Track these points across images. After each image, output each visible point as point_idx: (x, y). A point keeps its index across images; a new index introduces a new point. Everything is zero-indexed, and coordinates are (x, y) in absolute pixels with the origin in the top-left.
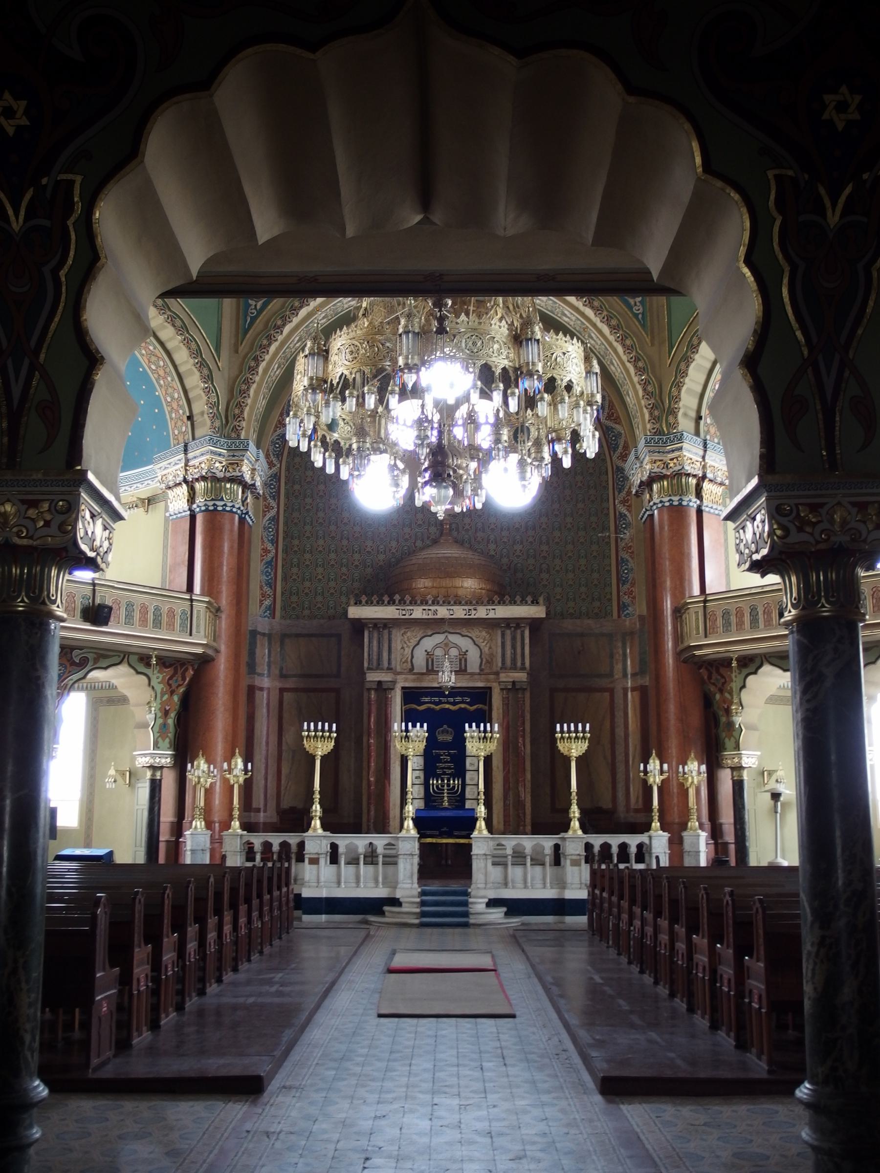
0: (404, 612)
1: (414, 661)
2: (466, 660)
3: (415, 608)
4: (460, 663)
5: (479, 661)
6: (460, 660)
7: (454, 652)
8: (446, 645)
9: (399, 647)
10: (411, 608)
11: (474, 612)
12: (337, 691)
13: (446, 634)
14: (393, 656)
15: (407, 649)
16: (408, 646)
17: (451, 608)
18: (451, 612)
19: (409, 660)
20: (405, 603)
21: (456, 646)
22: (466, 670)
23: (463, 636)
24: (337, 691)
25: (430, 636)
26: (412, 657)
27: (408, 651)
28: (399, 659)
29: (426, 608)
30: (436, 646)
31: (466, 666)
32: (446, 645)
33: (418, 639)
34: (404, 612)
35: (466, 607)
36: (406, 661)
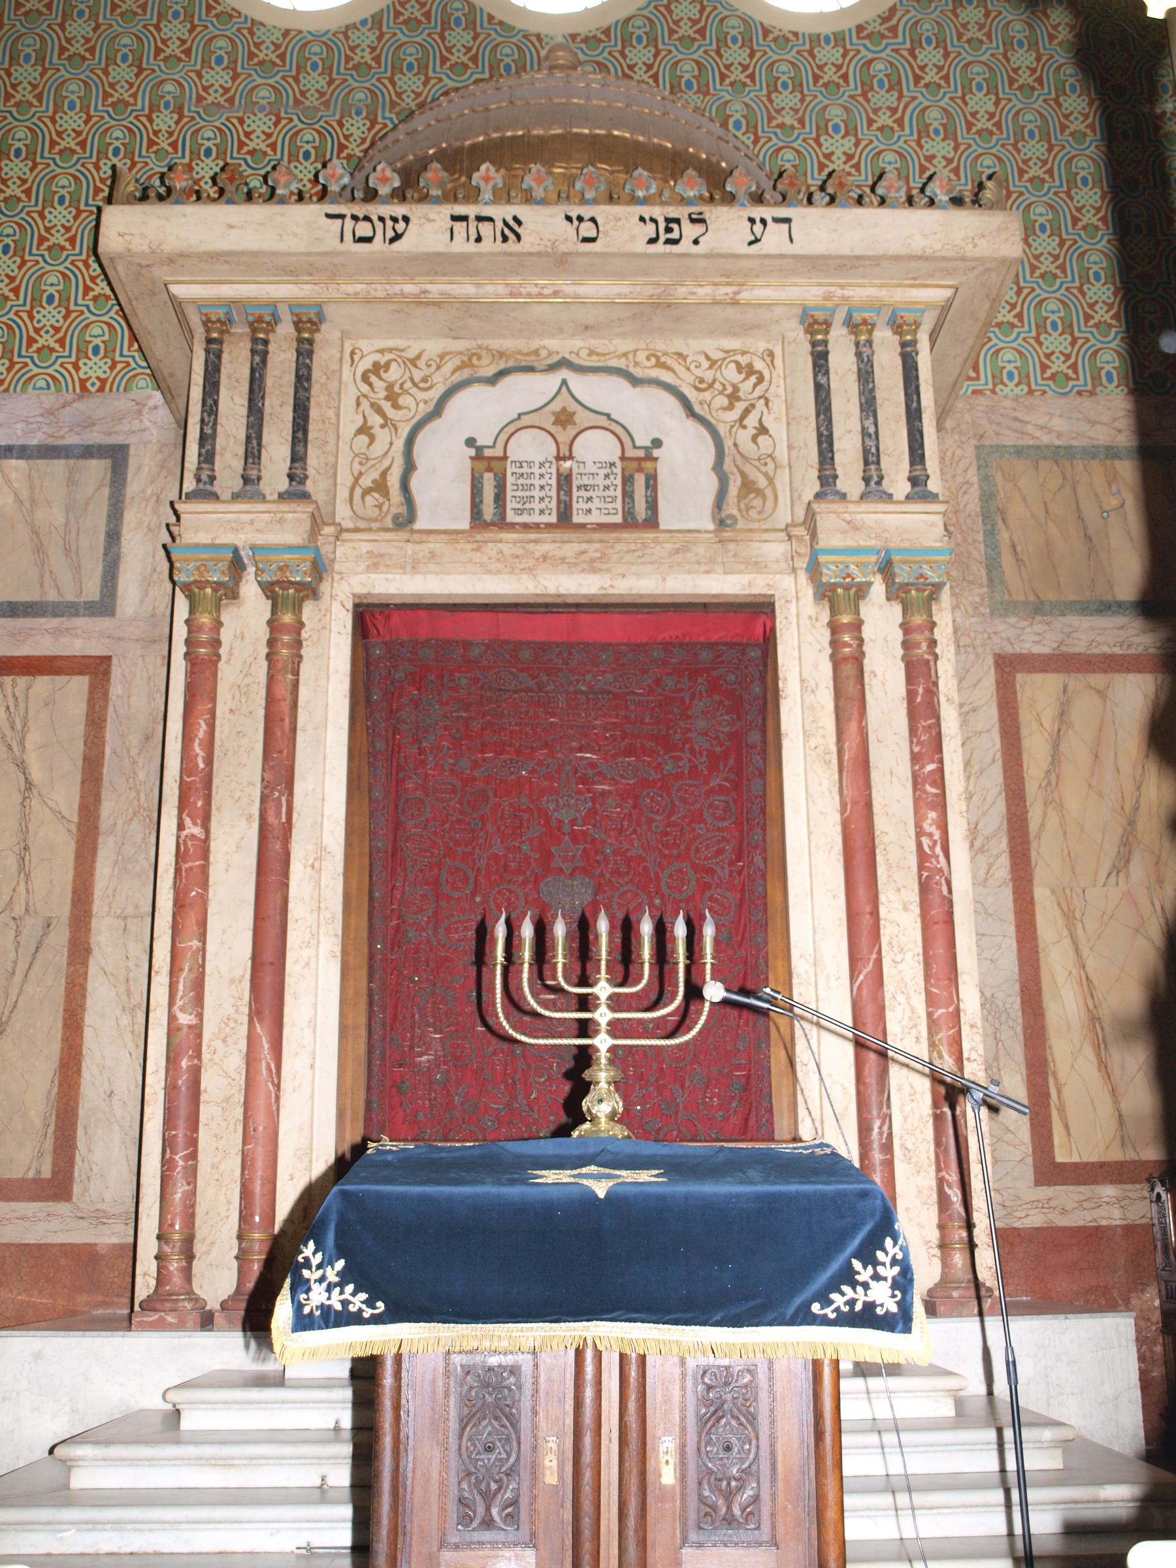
0: (364, 229)
1: (415, 483)
2: (652, 482)
3: (416, 211)
4: (628, 495)
5: (711, 484)
6: (627, 480)
7: (596, 450)
8: (564, 419)
9: (350, 422)
10: (399, 210)
11: (690, 231)
12: (97, 669)
13: (564, 373)
14: (314, 458)
15: (383, 436)
16: (387, 422)
17: (587, 211)
18: (587, 230)
19: (394, 480)
20: (371, 195)
21: (609, 423)
22: (652, 523)
23: (635, 381)
24: (97, 669)
25: (493, 380)
26: (410, 466)
27: (387, 446)
28: (344, 479)
29: (470, 210)
30: (516, 426)
31: (653, 506)
32: (564, 419)
33: (435, 394)
34: (364, 229)
35: (658, 212)
36: (381, 486)
